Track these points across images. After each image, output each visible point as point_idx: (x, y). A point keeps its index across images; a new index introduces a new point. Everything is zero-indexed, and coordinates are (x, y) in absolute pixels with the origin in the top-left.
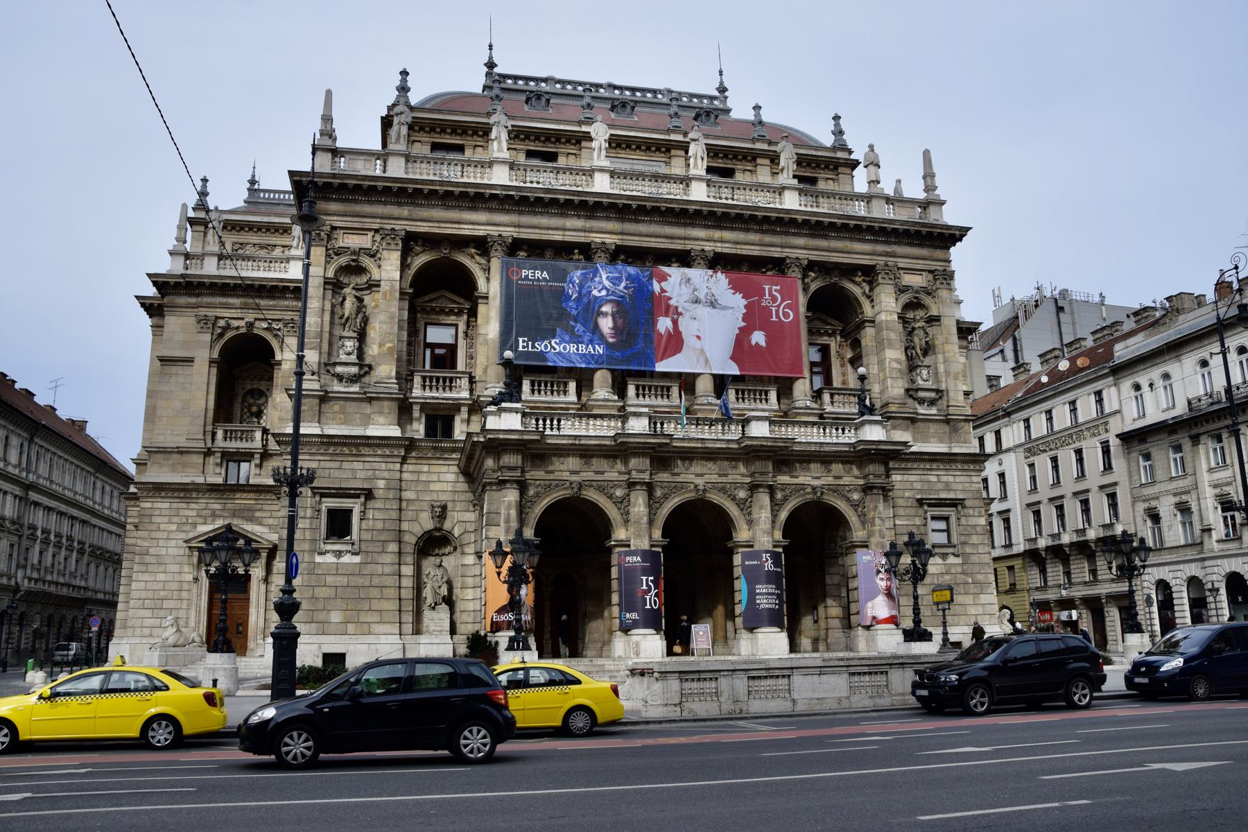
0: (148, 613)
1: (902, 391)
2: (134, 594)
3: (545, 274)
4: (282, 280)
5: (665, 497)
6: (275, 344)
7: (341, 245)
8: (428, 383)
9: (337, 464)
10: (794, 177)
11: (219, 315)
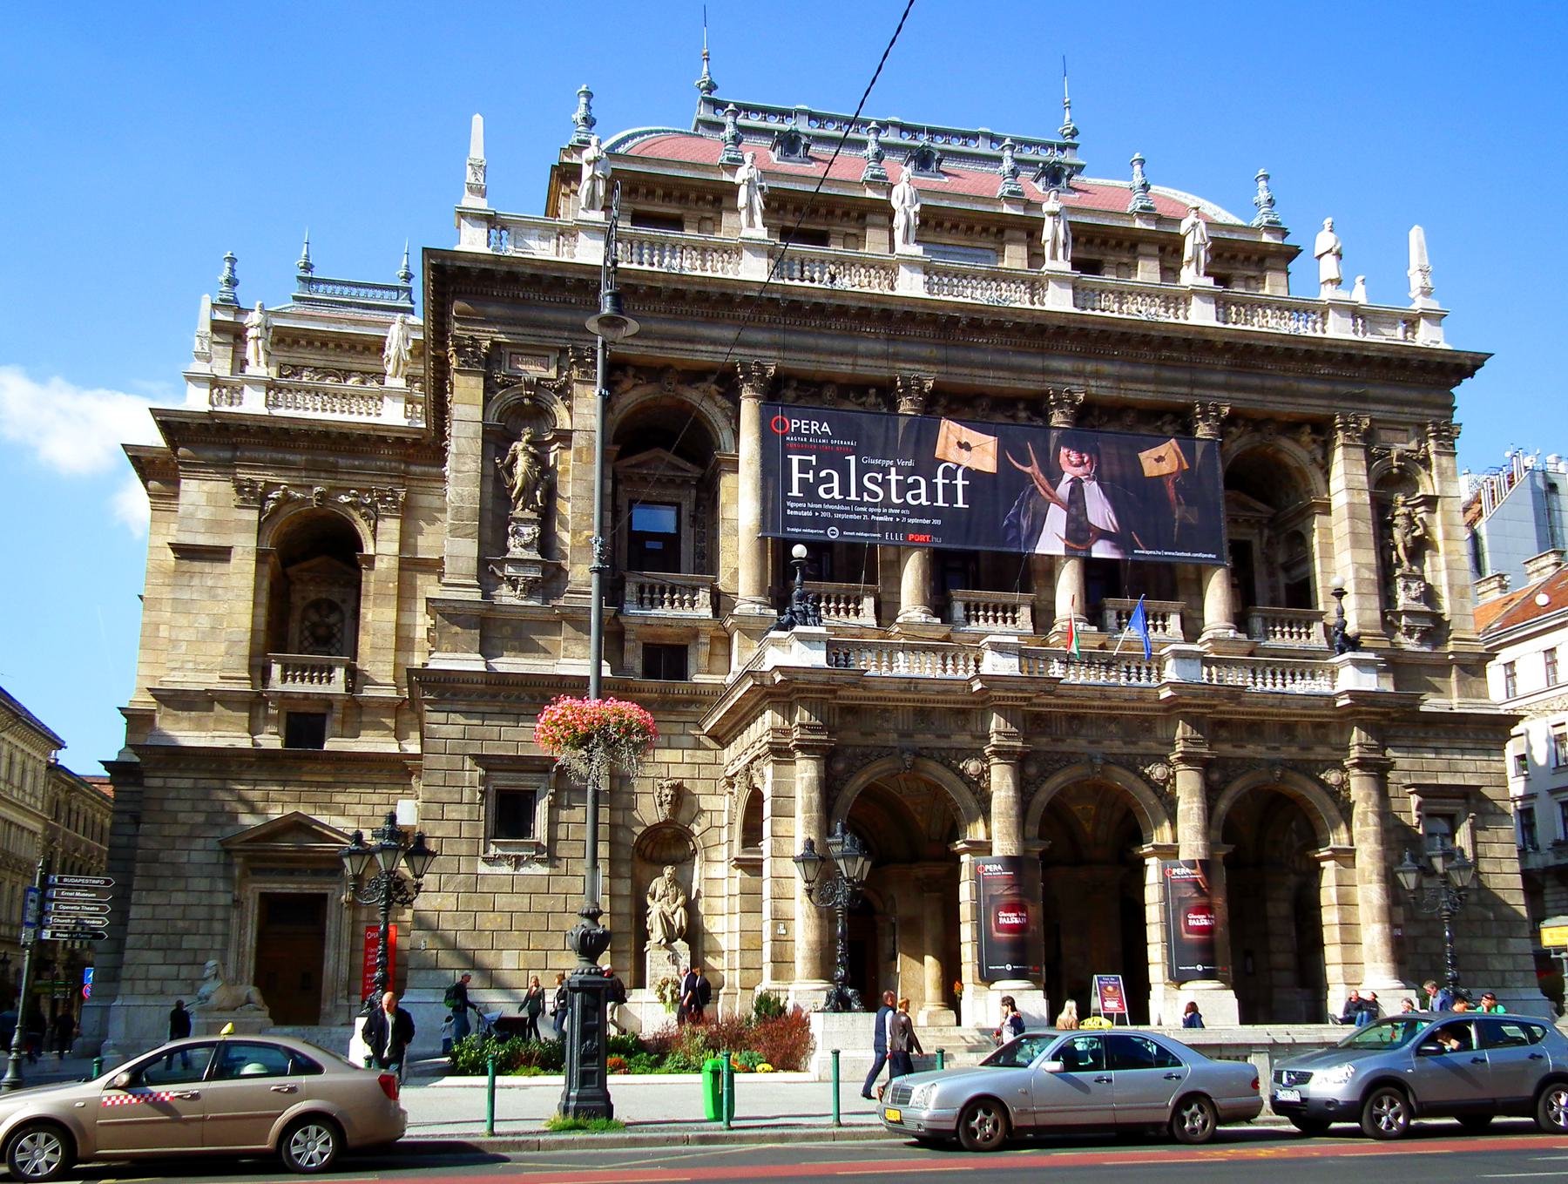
0: (156, 957)
1: (1377, 615)
2: (133, 926)
3: (826, 428)
4: (375, 426)
5: (1044, 775)
6: (363, 528)
10: (1207, 274)
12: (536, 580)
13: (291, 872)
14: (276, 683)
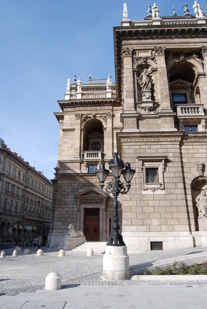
0: (61, 223)
7: (138, 56)
8: (184, 111)
9: (149, 146)
11: (83, 113)
12: (151, 107)
13: (91, 203)
14: (85, 157)
